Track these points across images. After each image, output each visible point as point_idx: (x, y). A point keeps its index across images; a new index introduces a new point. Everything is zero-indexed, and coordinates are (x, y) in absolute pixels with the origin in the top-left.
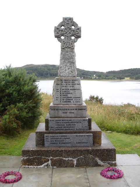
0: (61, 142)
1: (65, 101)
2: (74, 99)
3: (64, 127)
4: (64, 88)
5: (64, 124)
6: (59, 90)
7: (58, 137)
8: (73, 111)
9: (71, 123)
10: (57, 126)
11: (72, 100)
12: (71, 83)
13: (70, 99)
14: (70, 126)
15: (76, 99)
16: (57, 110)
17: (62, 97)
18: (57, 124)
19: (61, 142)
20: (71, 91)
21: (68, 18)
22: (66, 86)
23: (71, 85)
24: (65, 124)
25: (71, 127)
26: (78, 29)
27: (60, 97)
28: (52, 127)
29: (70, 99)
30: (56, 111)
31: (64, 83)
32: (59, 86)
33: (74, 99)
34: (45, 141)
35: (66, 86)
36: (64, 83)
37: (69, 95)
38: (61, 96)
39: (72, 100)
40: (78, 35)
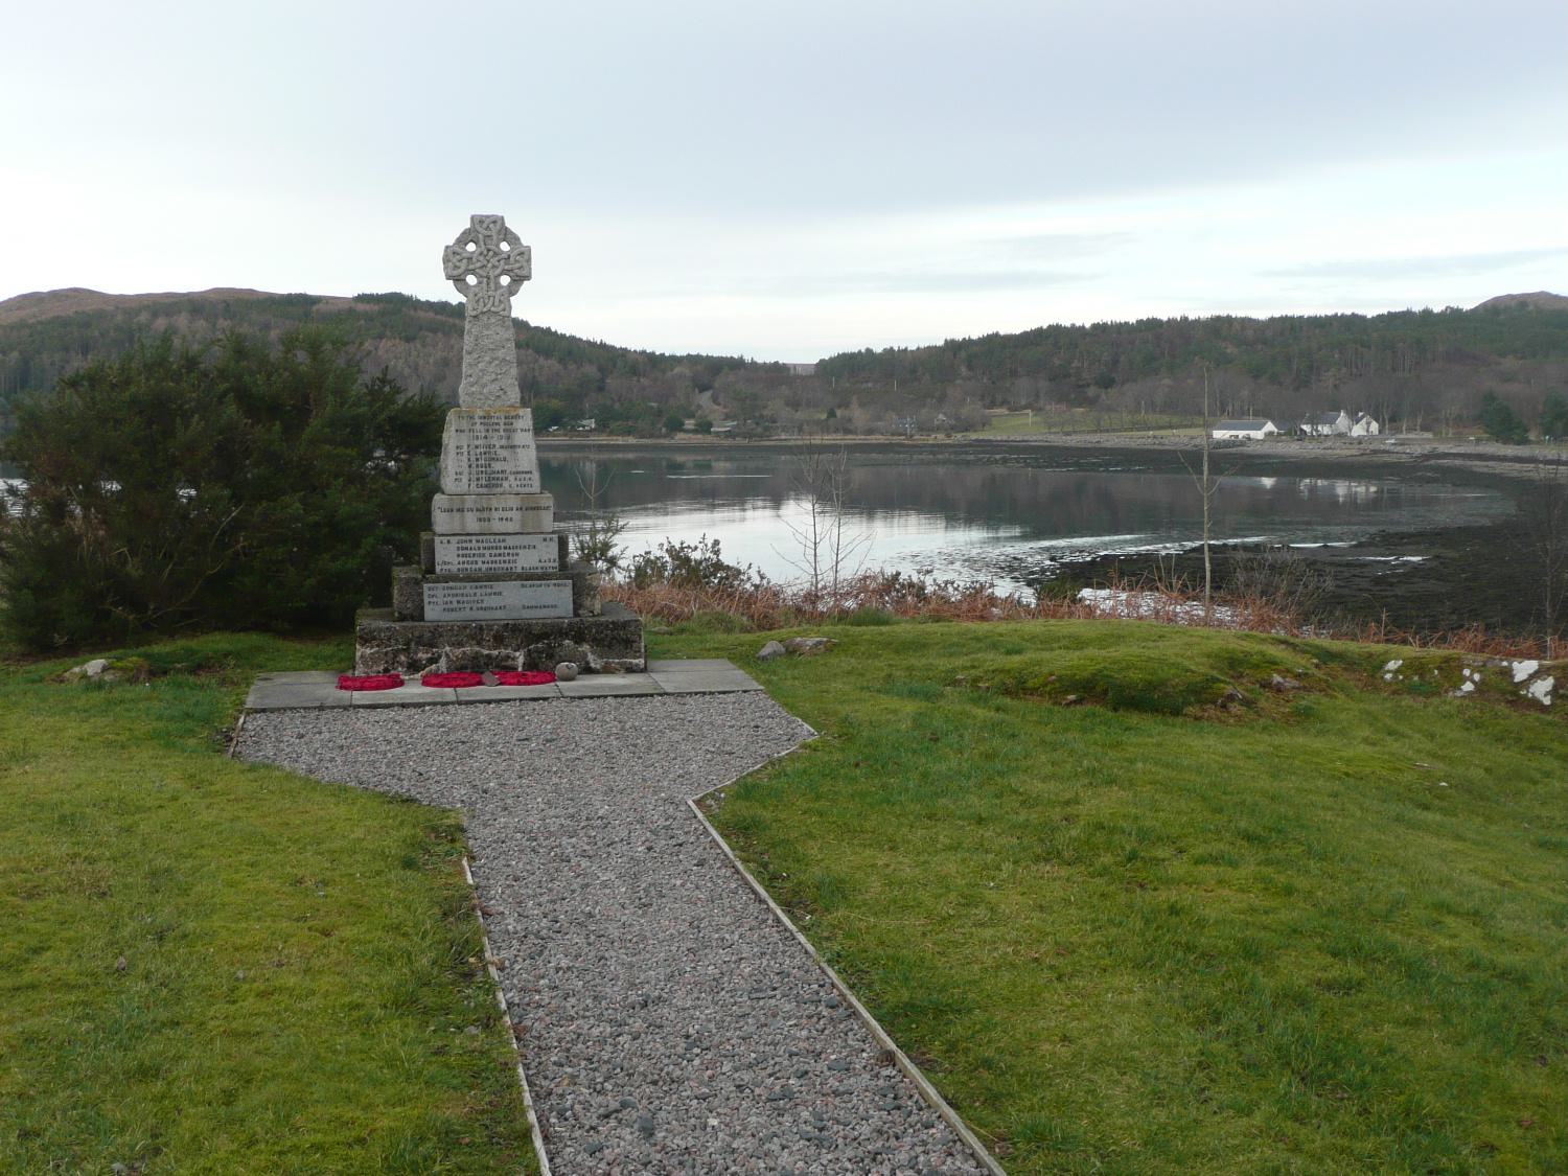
0: (475, 606)
1: (484, 482)
2: (512, 478)
3: (483, 563)
4: (480, 442)
5: (482, 551)
6: (465, 449)
7: (465, 591)
8: (509, 514)
9: (505, 548)
10: (461, 559)
11: (506, 479)
12: (502, 427)
13: (500, 476)
14: (502, 558)
15: (519, 476)
16: (458, 510)
17: (474, 470)
18: (461, 552)
19: (475, 606)
20: (503, 453)
21: (488, 217)
22: (486, 437)
23: (502, 433)
24: (487, 552)
25: (505, 562)
26: (522, 254)
27: (466, 470)
28: (445, 563)
29: (500, 476)
30: (457, 515)
31: (478, 427)
32: (464, 436)
33: (512, 478)
34: (426, 600)
35: (486, 437)
36: (478, 427)
37: (497, 466)
38: (470, 466)
39: (506, 479)
40: (524, 273)
